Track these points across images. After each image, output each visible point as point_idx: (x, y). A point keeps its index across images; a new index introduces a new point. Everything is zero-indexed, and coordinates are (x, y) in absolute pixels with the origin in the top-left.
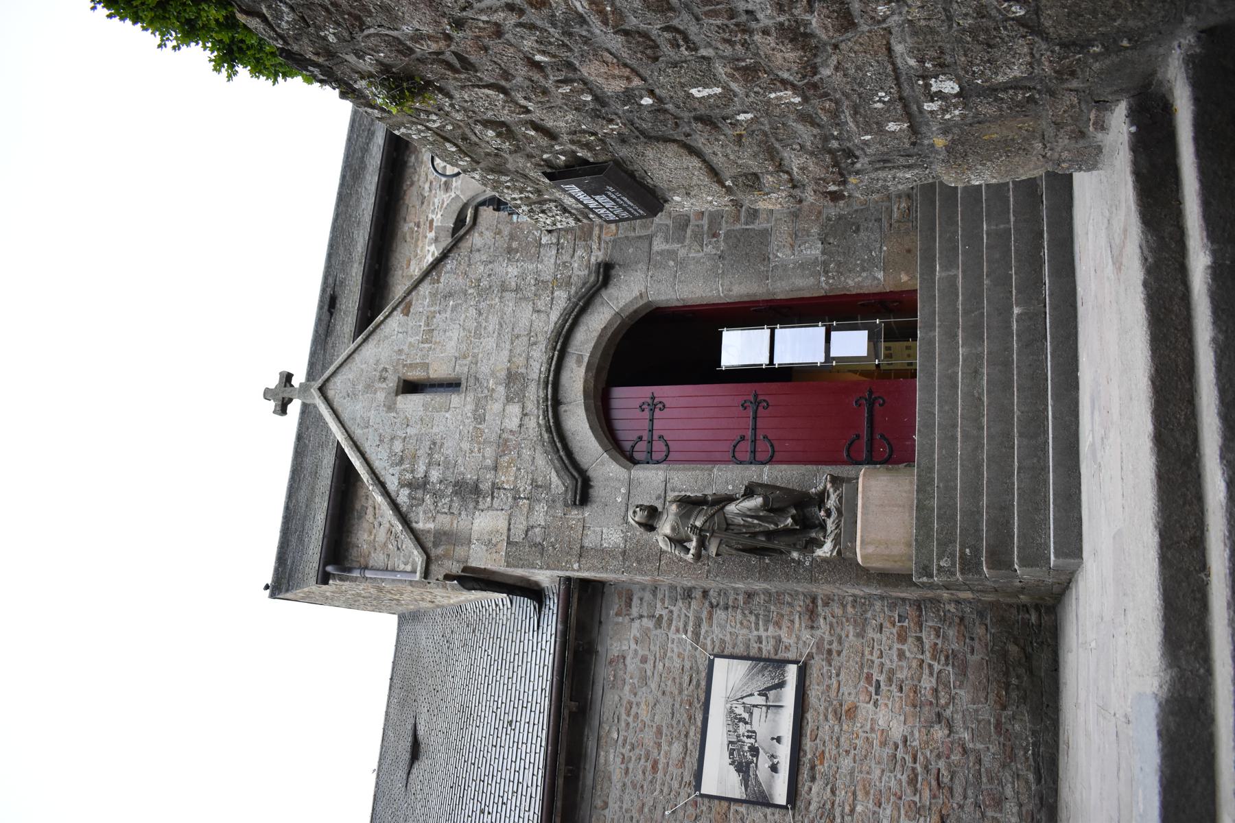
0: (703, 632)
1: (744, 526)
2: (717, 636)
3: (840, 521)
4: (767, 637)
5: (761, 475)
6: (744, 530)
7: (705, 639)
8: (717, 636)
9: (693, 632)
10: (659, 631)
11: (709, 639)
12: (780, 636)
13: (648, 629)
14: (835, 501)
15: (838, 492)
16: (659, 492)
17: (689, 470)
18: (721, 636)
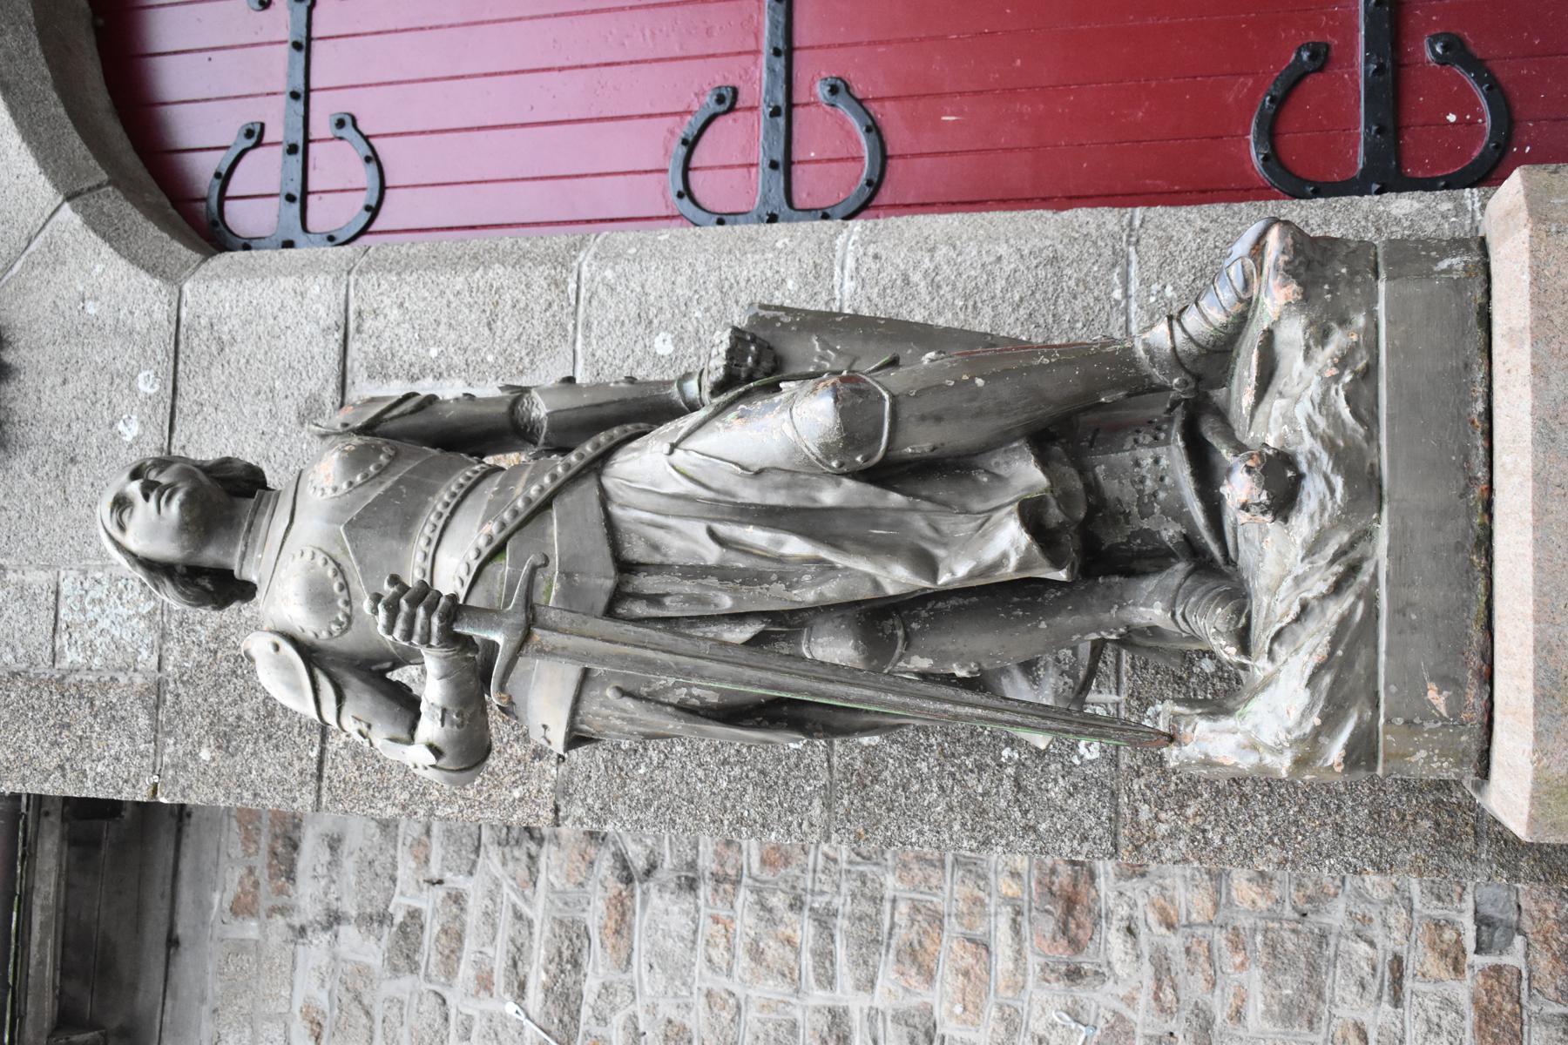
0: (591, 987)
1: (722, 573)
2: (652, 1009)
3: (1366, 535)
4: (872, 1016)
5: (820, 273)
6: (726, 603)
7: (602, 1020)
8: (652, 1009)
9: (548, 990)
10: (406, 982)
11: (618, 1020)
12: (928, 1011)
13: (363, 972)
14: (1324, 403)
15: (1339, 340)
16: (311, 386)
17: (455, 265)
18: (667, 1009)
